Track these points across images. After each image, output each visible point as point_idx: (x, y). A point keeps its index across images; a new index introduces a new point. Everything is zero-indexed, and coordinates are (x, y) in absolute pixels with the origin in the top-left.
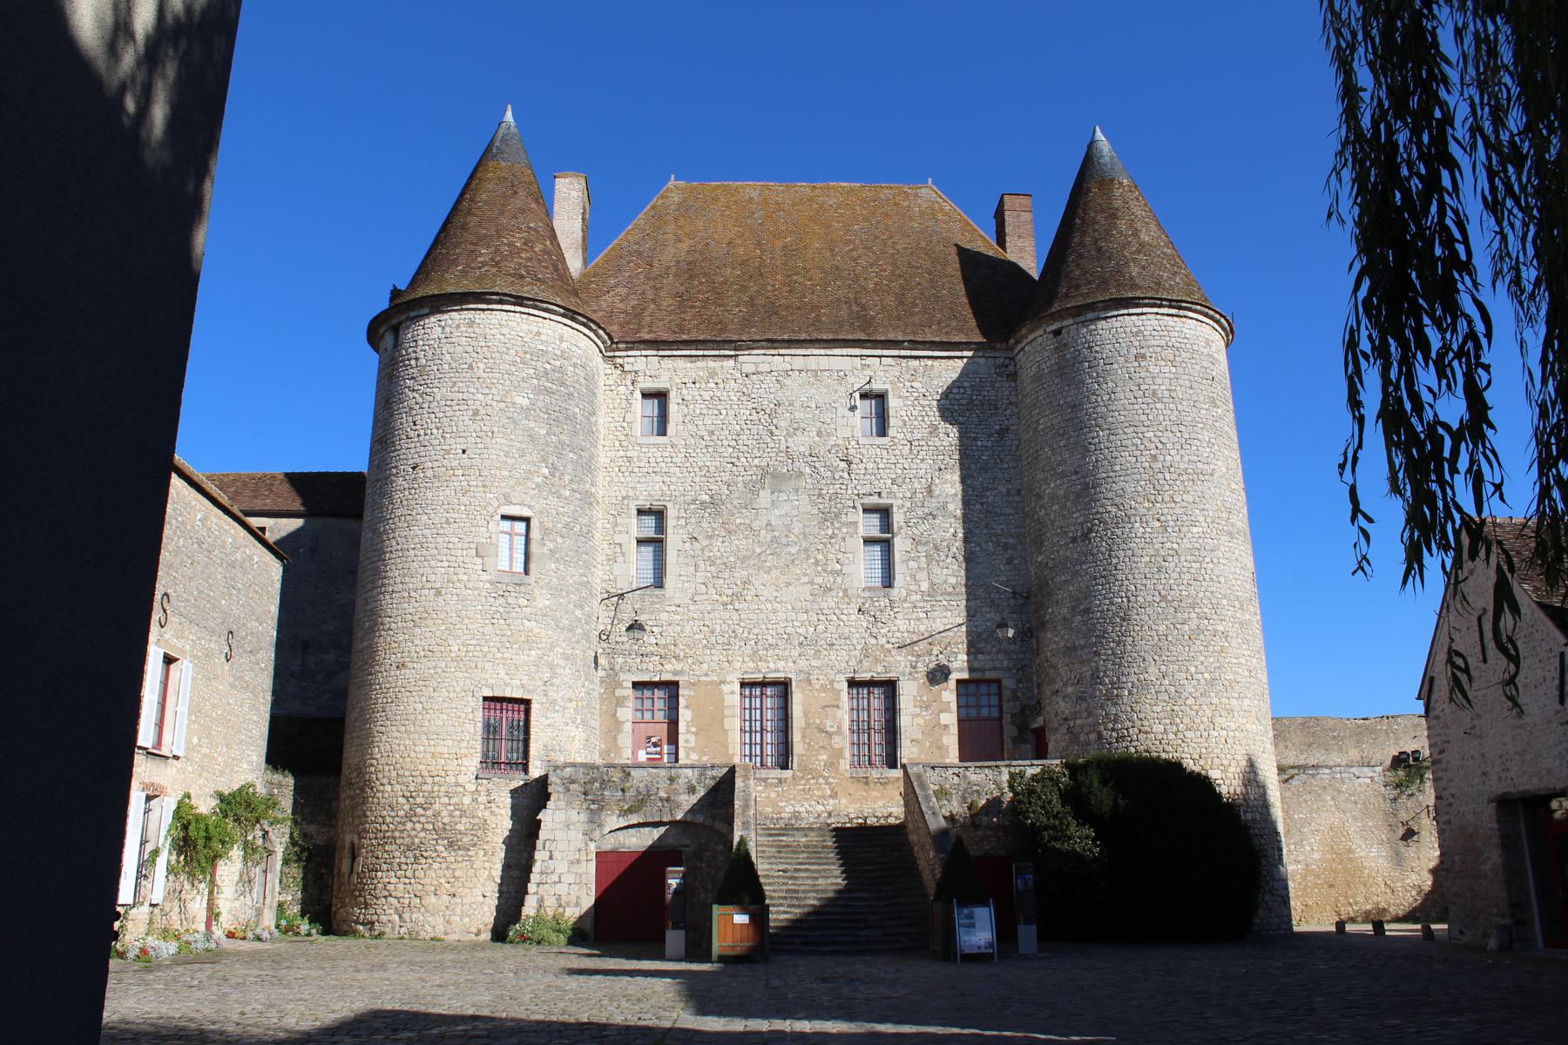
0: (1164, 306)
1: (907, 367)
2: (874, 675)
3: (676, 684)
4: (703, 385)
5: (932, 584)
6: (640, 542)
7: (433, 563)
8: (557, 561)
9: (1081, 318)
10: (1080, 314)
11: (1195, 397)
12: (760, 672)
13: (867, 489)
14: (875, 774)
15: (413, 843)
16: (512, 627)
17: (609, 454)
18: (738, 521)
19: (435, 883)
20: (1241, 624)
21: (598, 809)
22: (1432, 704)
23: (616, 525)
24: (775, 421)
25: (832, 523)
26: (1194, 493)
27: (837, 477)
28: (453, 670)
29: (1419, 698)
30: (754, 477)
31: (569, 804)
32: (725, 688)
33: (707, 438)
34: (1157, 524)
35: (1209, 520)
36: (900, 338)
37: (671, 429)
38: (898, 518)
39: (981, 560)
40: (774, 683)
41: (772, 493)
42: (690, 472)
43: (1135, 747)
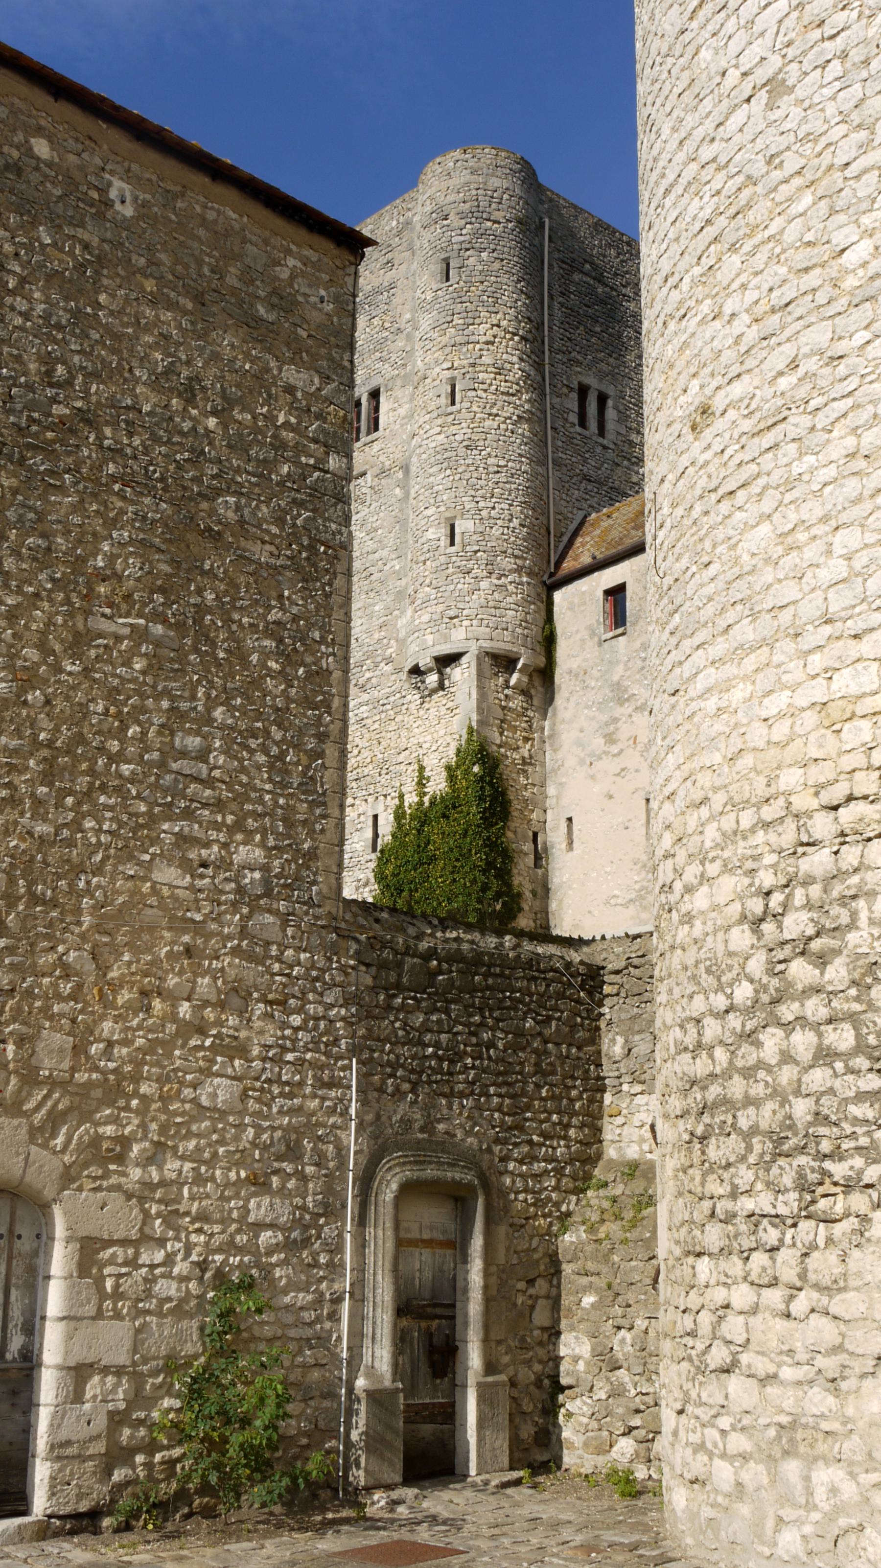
15: (789, 1123)
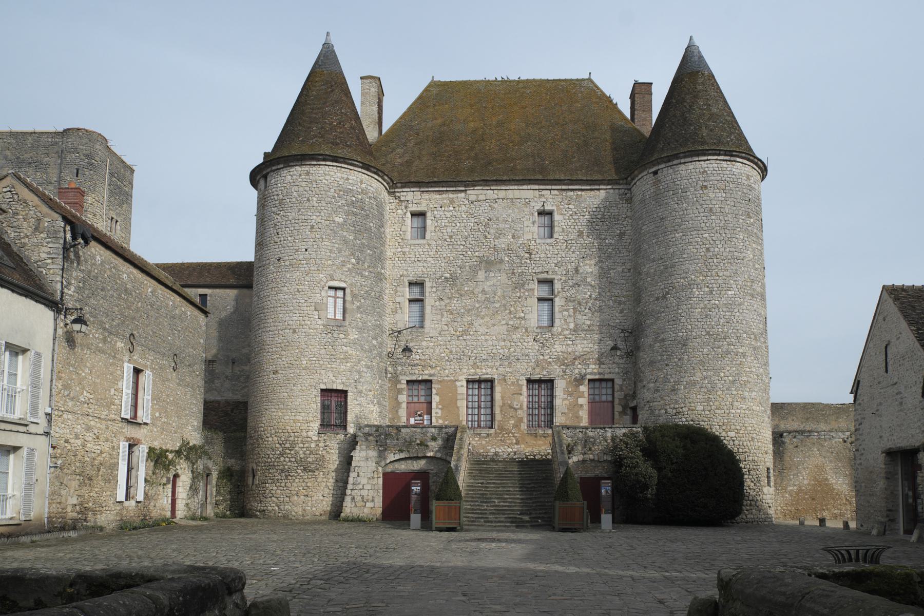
0: (721, 155)
1: (566, 196)
2: (542, 376)
3: (431, 381)
4: (446, 209)
5: (576, 325)
6: (410, 301)
7: (291, 315)
8: (361, 313)
9: (670, 164)
10: (669, 161)
11: (736, 212)
12: (477, 374)
13: (540, 269)
14: (541, 432)
15: (285, 469)
16: (336, 350)
17: (392, 250)
18: (466, 289)
19: (297, 489)
20: (754, 348)
21: (383, 450)
22: (858, 397)
23: (397, 291)
24: (488, 229)
25: (520, 290)
26: (730, 271)
27: (523, 263)
28: (304, 374)
29: (851, 393)
30: (475, 263)
31: (368, 447)
32: (458, 384)
33: (448, 240)
34: (707, 289)
35: (739, 286)
36: (562, 178)
37: (428, 235)
38: (557, 286)
39: (605, 310)
40: (486, 381)
41: (486, 272)
42: (438, 260)
43: (686, 418)
